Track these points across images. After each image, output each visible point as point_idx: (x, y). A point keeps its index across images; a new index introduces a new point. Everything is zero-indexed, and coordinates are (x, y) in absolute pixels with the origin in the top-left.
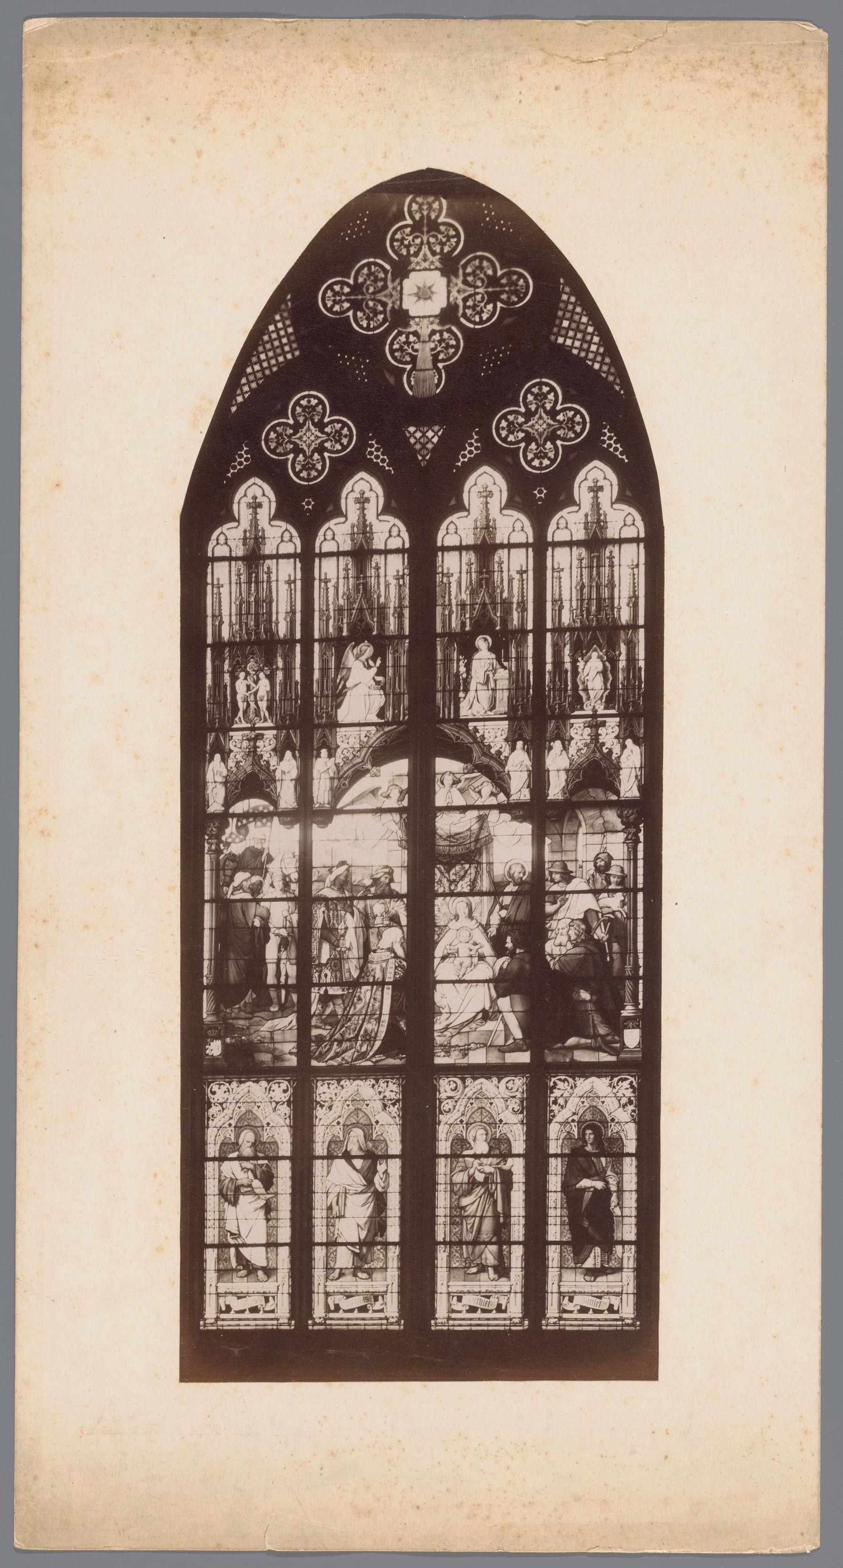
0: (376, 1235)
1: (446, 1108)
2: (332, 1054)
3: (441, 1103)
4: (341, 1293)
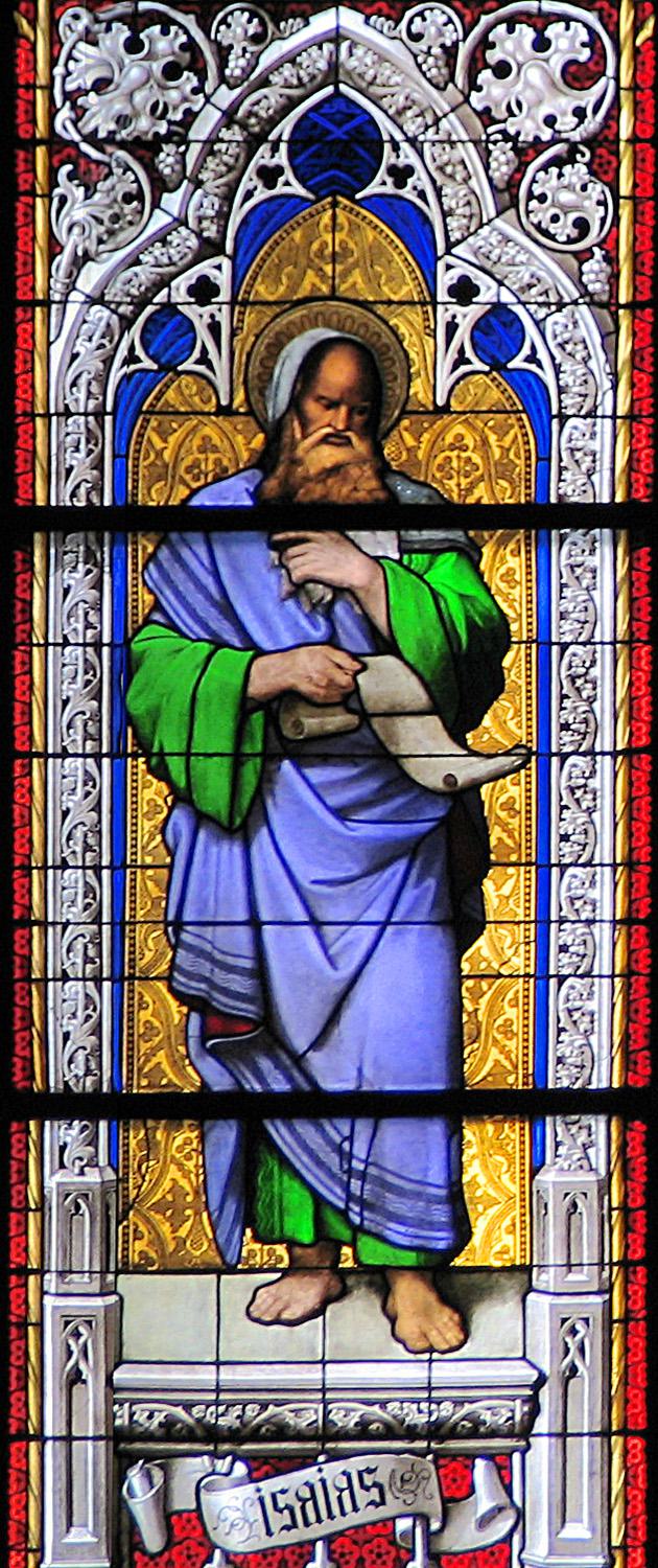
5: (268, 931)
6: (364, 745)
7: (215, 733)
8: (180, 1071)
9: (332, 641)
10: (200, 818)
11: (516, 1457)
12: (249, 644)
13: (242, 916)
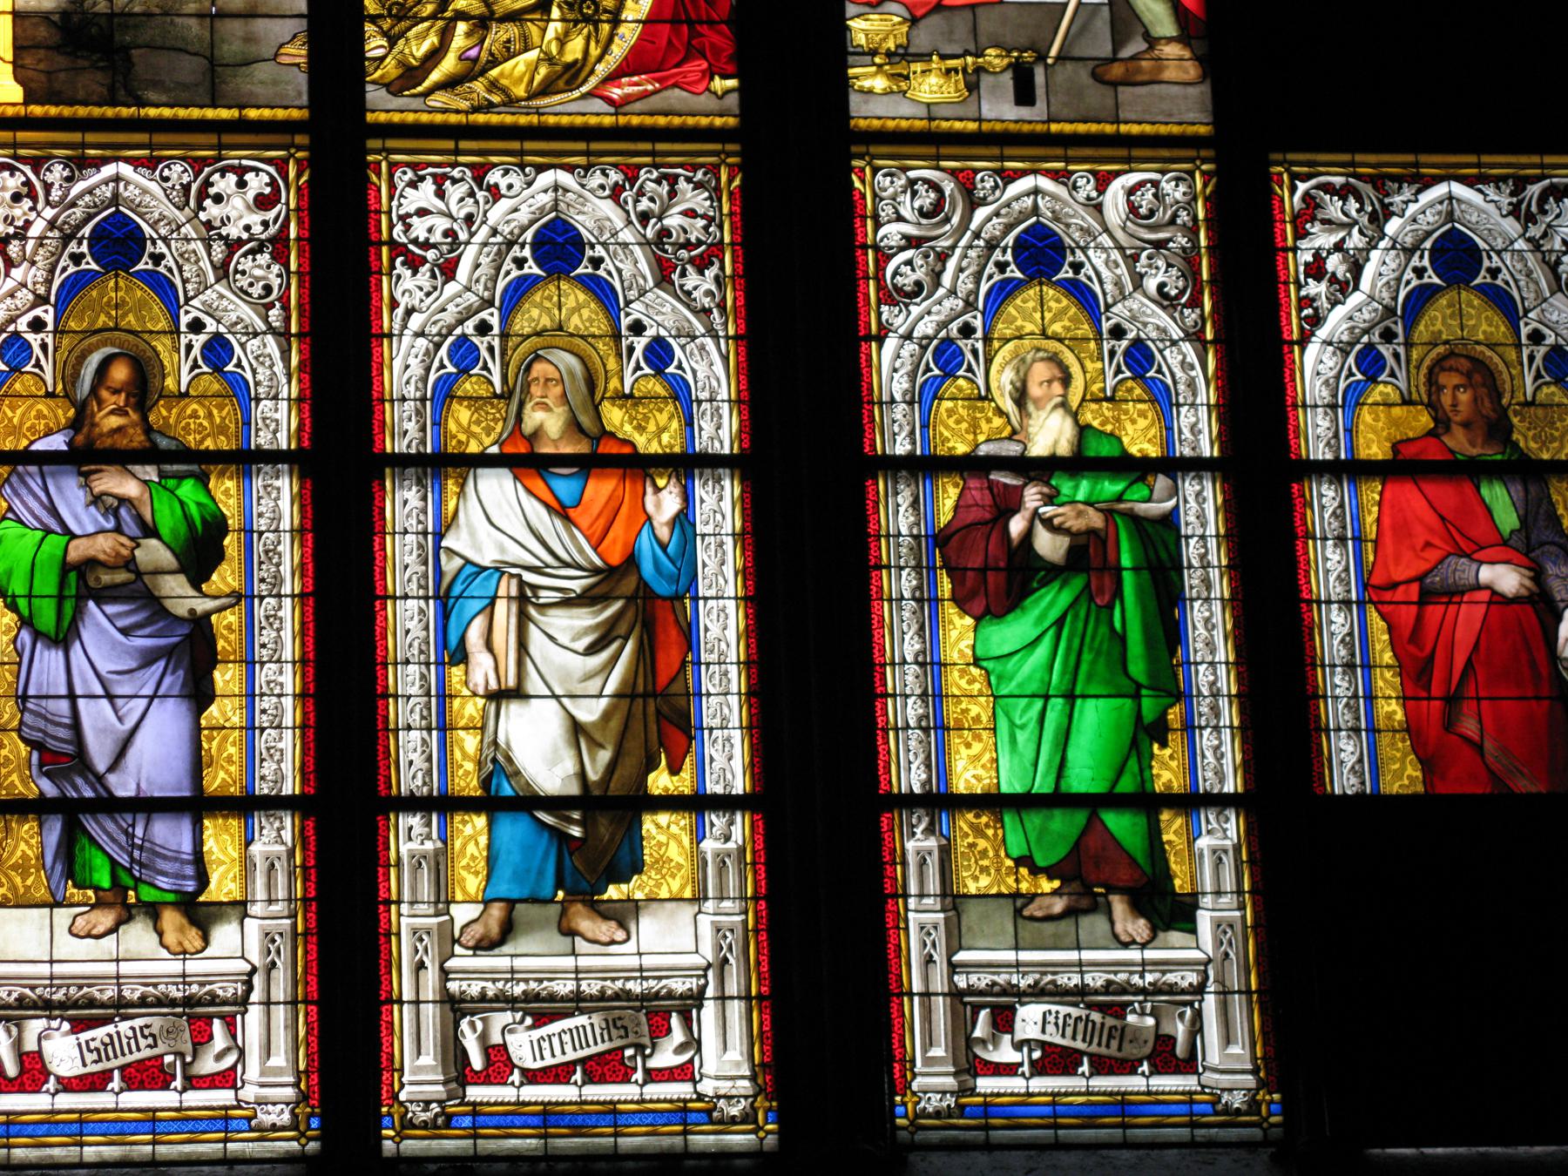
0: (652, 765)
1: (908, 280)
2: (449, 65)
3: (883, 257)
4: (506, 1001)
5: (81, 703)
6: (138, 591)
7: (47, 583)
8: (26, 785)
9: (118, 529)
10: (37, 635)
11: (239, 1017)
12: (67, 531)
13: (63, 691)
